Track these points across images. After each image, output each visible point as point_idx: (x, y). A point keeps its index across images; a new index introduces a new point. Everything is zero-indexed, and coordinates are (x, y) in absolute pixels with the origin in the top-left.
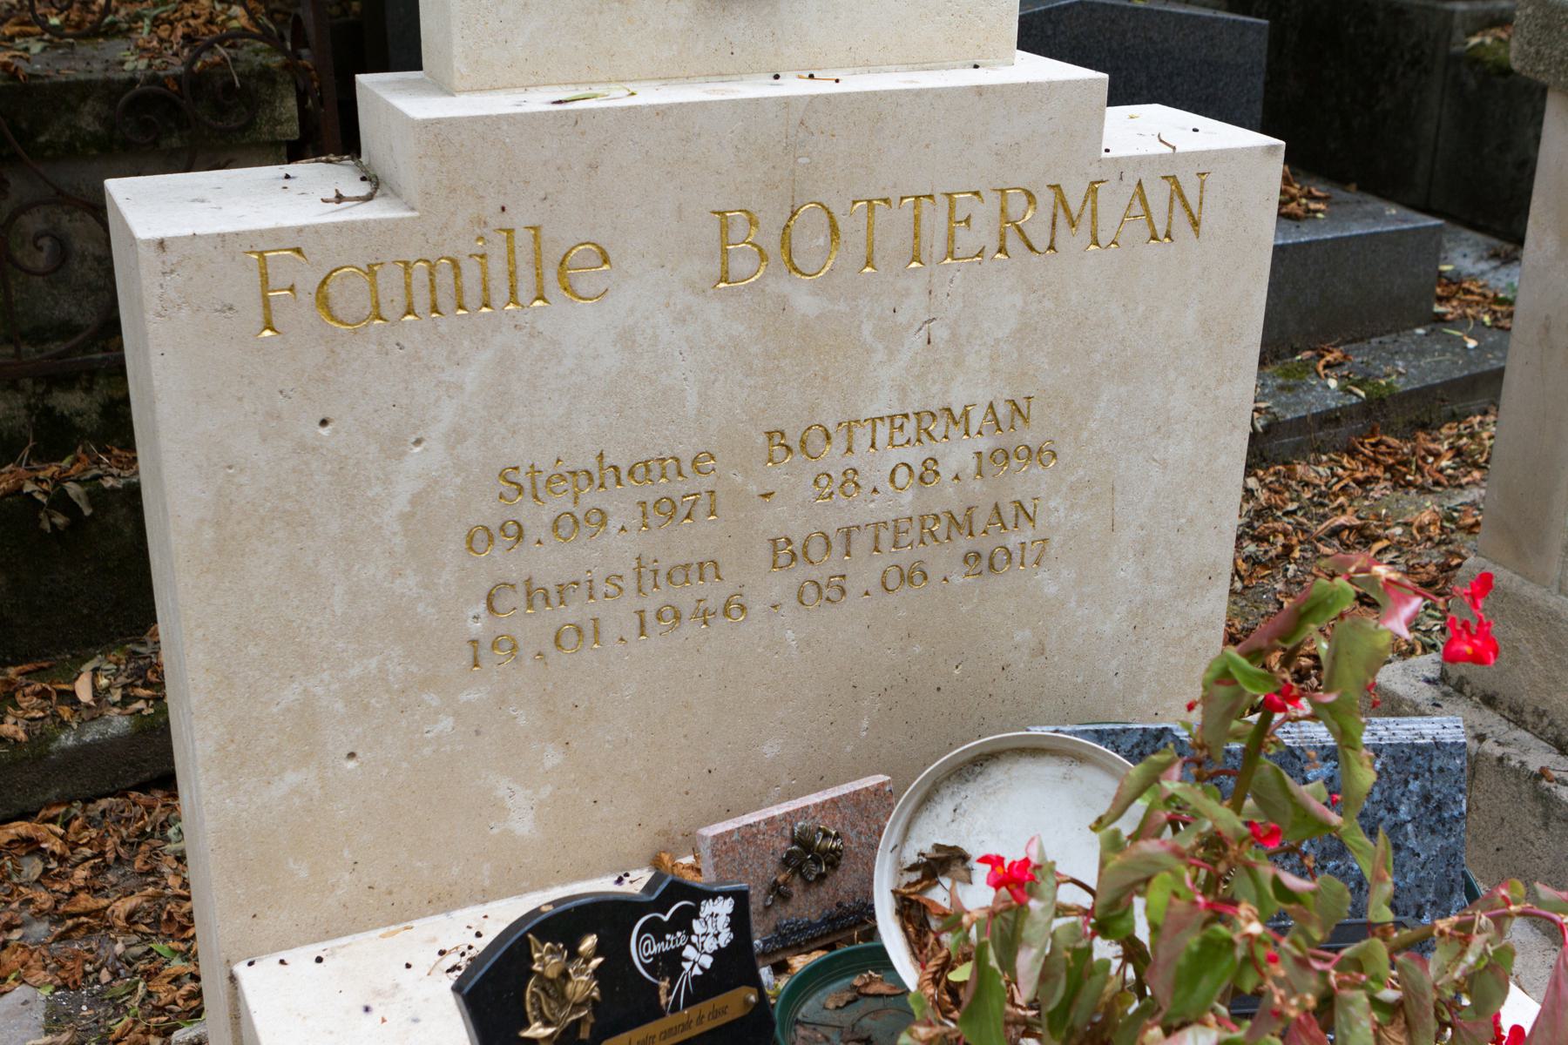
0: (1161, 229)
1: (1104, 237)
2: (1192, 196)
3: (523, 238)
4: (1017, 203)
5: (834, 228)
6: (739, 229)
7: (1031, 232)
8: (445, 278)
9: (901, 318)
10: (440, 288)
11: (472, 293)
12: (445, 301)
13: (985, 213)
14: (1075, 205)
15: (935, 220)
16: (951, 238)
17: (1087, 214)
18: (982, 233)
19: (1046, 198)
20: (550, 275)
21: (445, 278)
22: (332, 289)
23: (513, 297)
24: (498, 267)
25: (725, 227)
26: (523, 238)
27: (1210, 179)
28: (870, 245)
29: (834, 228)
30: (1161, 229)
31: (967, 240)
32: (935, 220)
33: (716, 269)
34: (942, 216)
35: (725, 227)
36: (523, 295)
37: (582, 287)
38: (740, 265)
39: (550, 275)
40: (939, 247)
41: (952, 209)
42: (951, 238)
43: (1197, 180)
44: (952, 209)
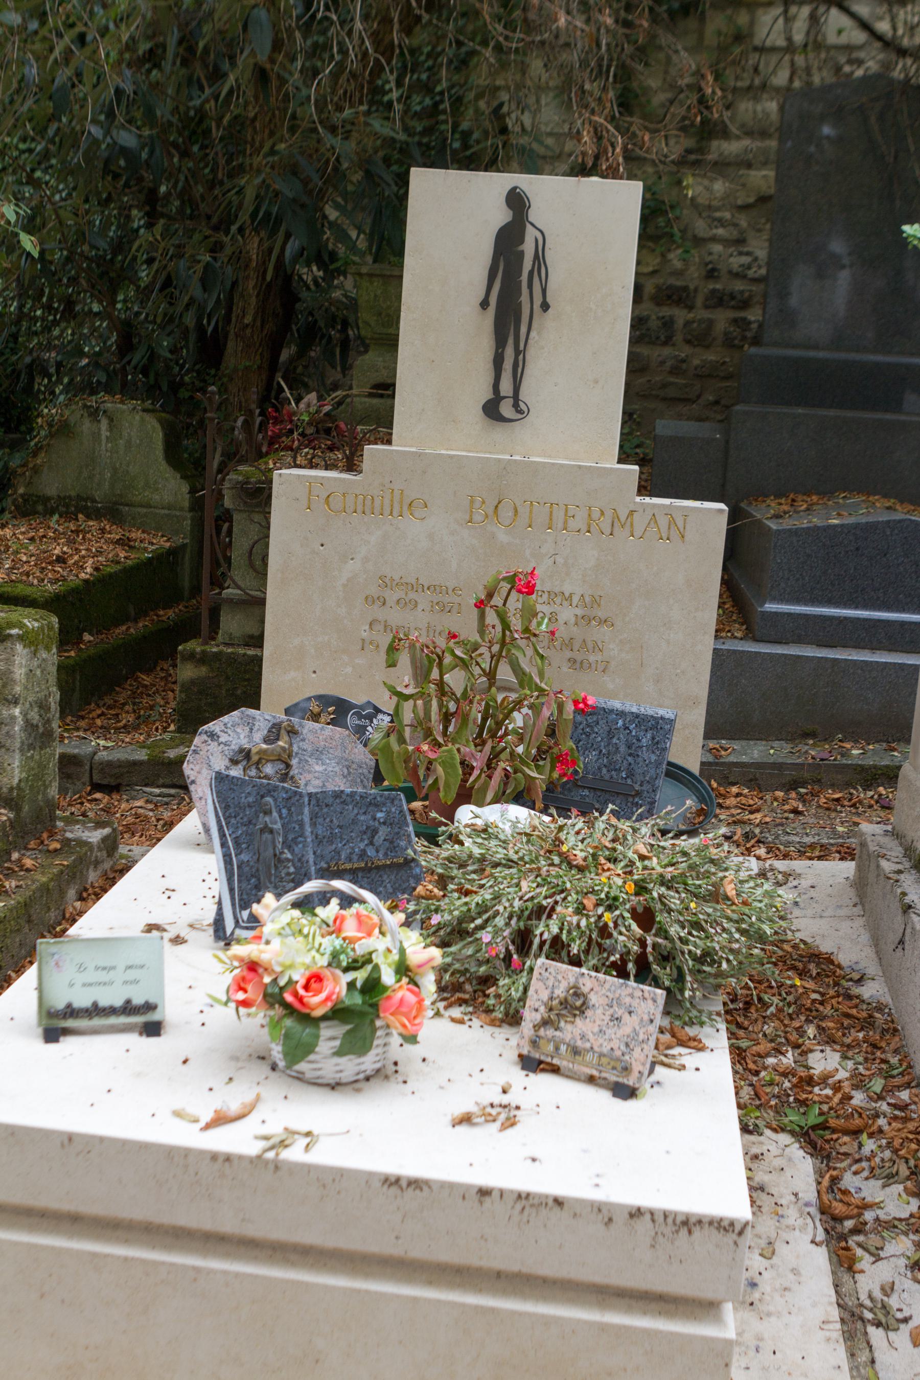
0: (664, 536)
1: (638, 533)
2: (680, 524)
3: (397, 493)
4: (596, 514)
5: (516, 511)
6: (477, 505)
7: (601, 525)
8: (368, 503)
9: (543, 551)
10: (367, 507)
11: (377, 509)
12: (367, 510)
13: (581, 514)
14: (623, 519)
15: (559, 515)
16: (565, 522)
17: (628, 524)
18: (578, 523)
19: (609, 513)
20: (405, 508)
21: (368, 503)
22: (331, 499)
23: (391, 514)
24: (387, 502)
25: (472, 502)
26: (397, 493)
27: (688, 519)
28: (530, 518)
29: (516, 511)
30: (664, 536)
31: (572, 524)
32: (559, 515)
33: (468, 518)
34: (562, 513)
35: (472, 502)
36: (395, 513)
37: (416, 514)
38: (477, 518)
39: (405, 508)
40: (560, 525)
41: (566, 510)
42: (565, 522)
43: (682, 518)
44: (566, 510)
